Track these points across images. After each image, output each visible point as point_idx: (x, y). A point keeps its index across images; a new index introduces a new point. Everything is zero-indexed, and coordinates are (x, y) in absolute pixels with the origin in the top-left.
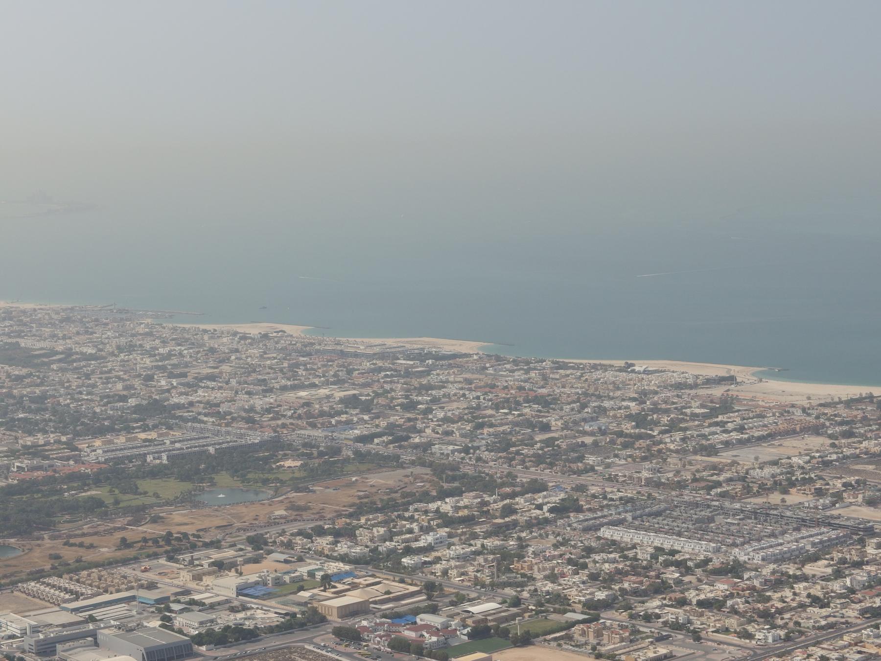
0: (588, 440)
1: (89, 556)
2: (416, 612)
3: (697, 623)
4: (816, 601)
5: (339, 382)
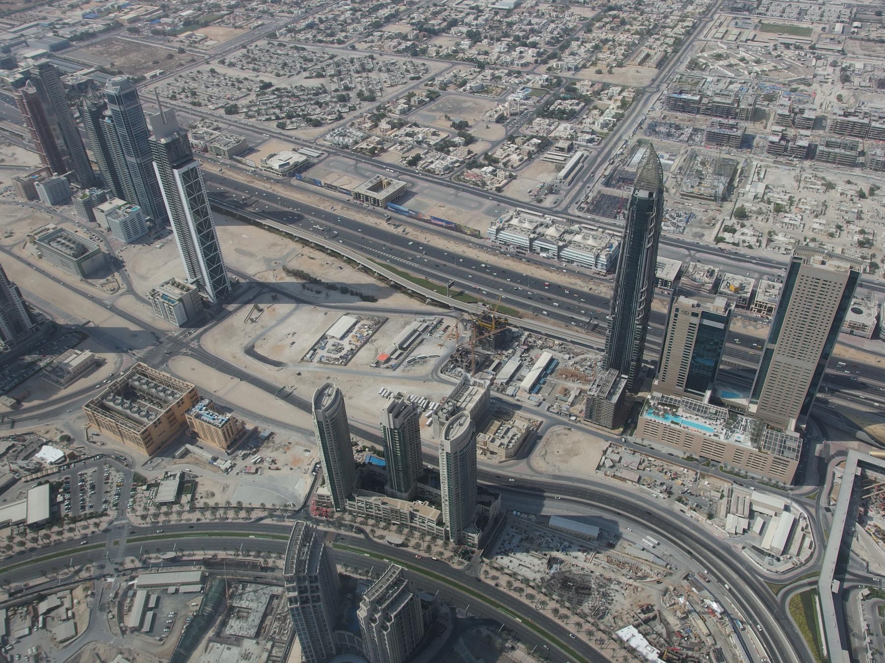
1: (13, 8)
2: (160, 17)
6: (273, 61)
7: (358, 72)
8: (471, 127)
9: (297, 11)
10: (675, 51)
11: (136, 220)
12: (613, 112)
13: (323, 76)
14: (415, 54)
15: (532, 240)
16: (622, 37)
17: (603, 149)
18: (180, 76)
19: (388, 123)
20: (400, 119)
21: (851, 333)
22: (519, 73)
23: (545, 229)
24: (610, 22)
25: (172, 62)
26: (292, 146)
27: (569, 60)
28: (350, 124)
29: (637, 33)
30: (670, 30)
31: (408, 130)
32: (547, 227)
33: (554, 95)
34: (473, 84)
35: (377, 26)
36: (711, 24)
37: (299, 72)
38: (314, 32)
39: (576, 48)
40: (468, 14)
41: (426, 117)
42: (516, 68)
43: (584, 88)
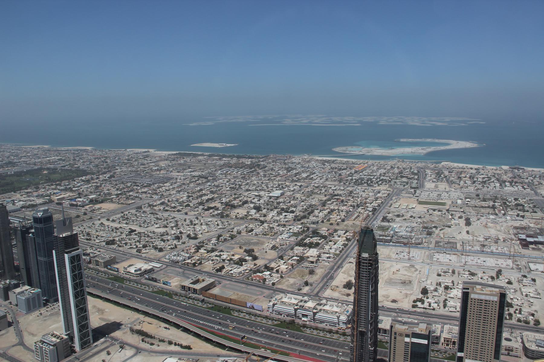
0: (117, 164)
3: (140, 196)
4: (166, 190)
5: (58, 156)
6: (138, 219)
7: (188, 225)
9: (155, 197)
11: (36, 298)
12: (342, 243)
13: (167, 227)
14: (222, 217)
15: (296, 310)
17: (337, 262)
19: (205, 250)
20: (212, 248)
21: (508, 354)
22: (285, 225)
23: (304, 304)
25: (79, 219)
26: (145, 261)
27: (312, 218)
29: (351, 206)
31: (217, 253)
32: (306, 302)
33: (306, 235)
36: (391, 202)
37: (153, 225)
39: (317, 213)
40: (254, 199)
42: (282, 223)
43: (323, 231)
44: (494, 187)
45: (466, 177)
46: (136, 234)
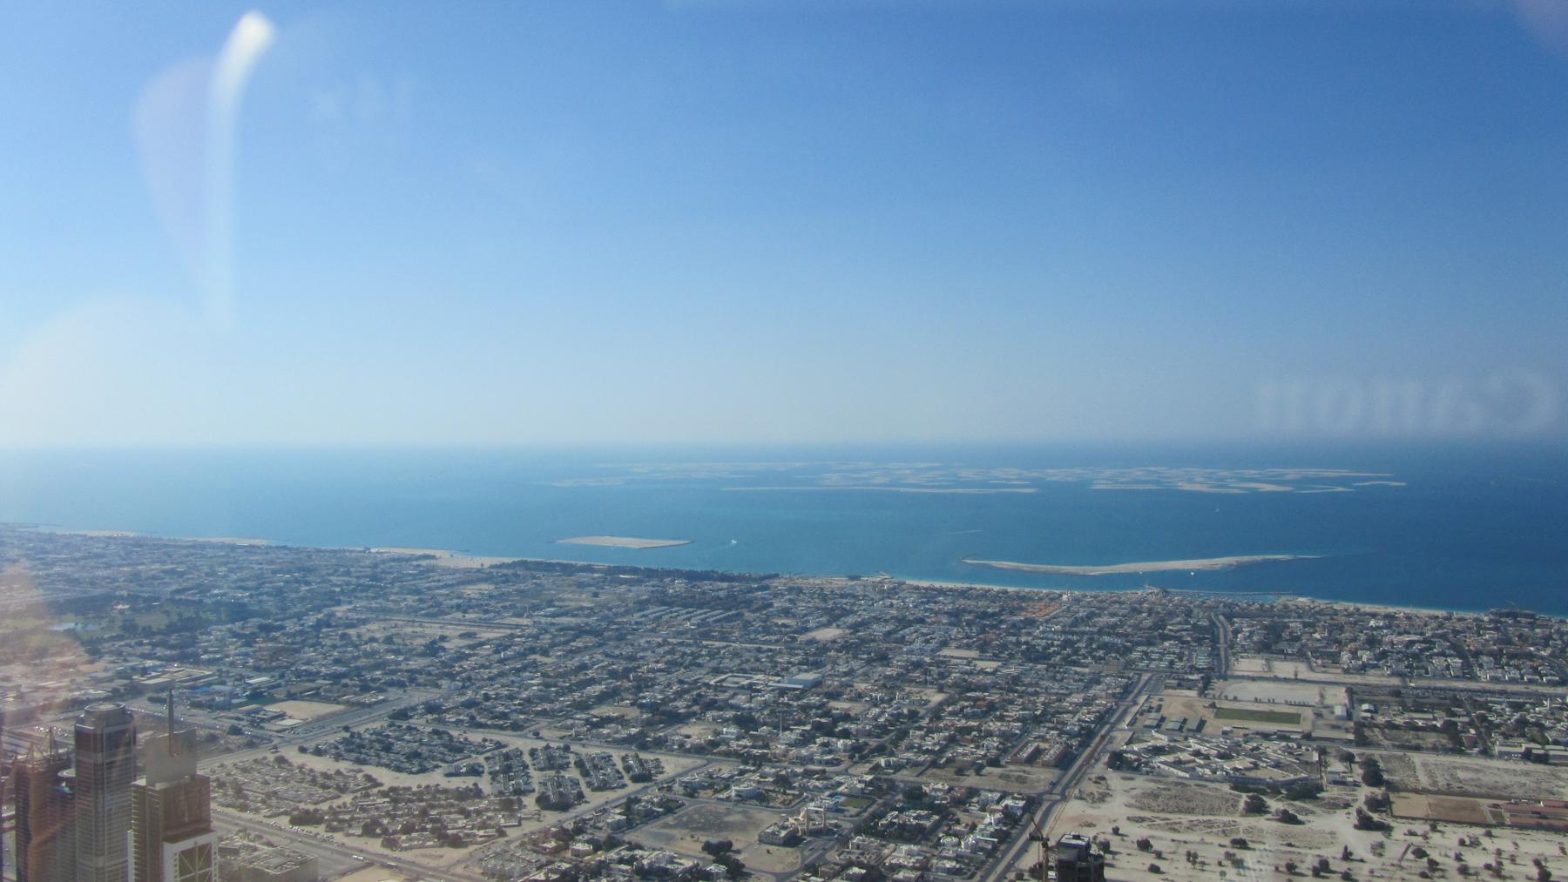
0: (338, 589)
5: (163, 562)
8: (738, 852)
10: (1084, 745)
14: (644, 747)
16: (994, 726)
18: (222, 766)
19: (588, 842)
24: (972, 707)
28: (517, 843)
29: (1018, 720)
30: (1071, 716)
33: (885, 804)
34: (742, 787)
35: (583, 706)
38: (473, 711)
41: (657, 836)
44: (1443, 673)
45: (1354, 640)
46: (384, 794)
